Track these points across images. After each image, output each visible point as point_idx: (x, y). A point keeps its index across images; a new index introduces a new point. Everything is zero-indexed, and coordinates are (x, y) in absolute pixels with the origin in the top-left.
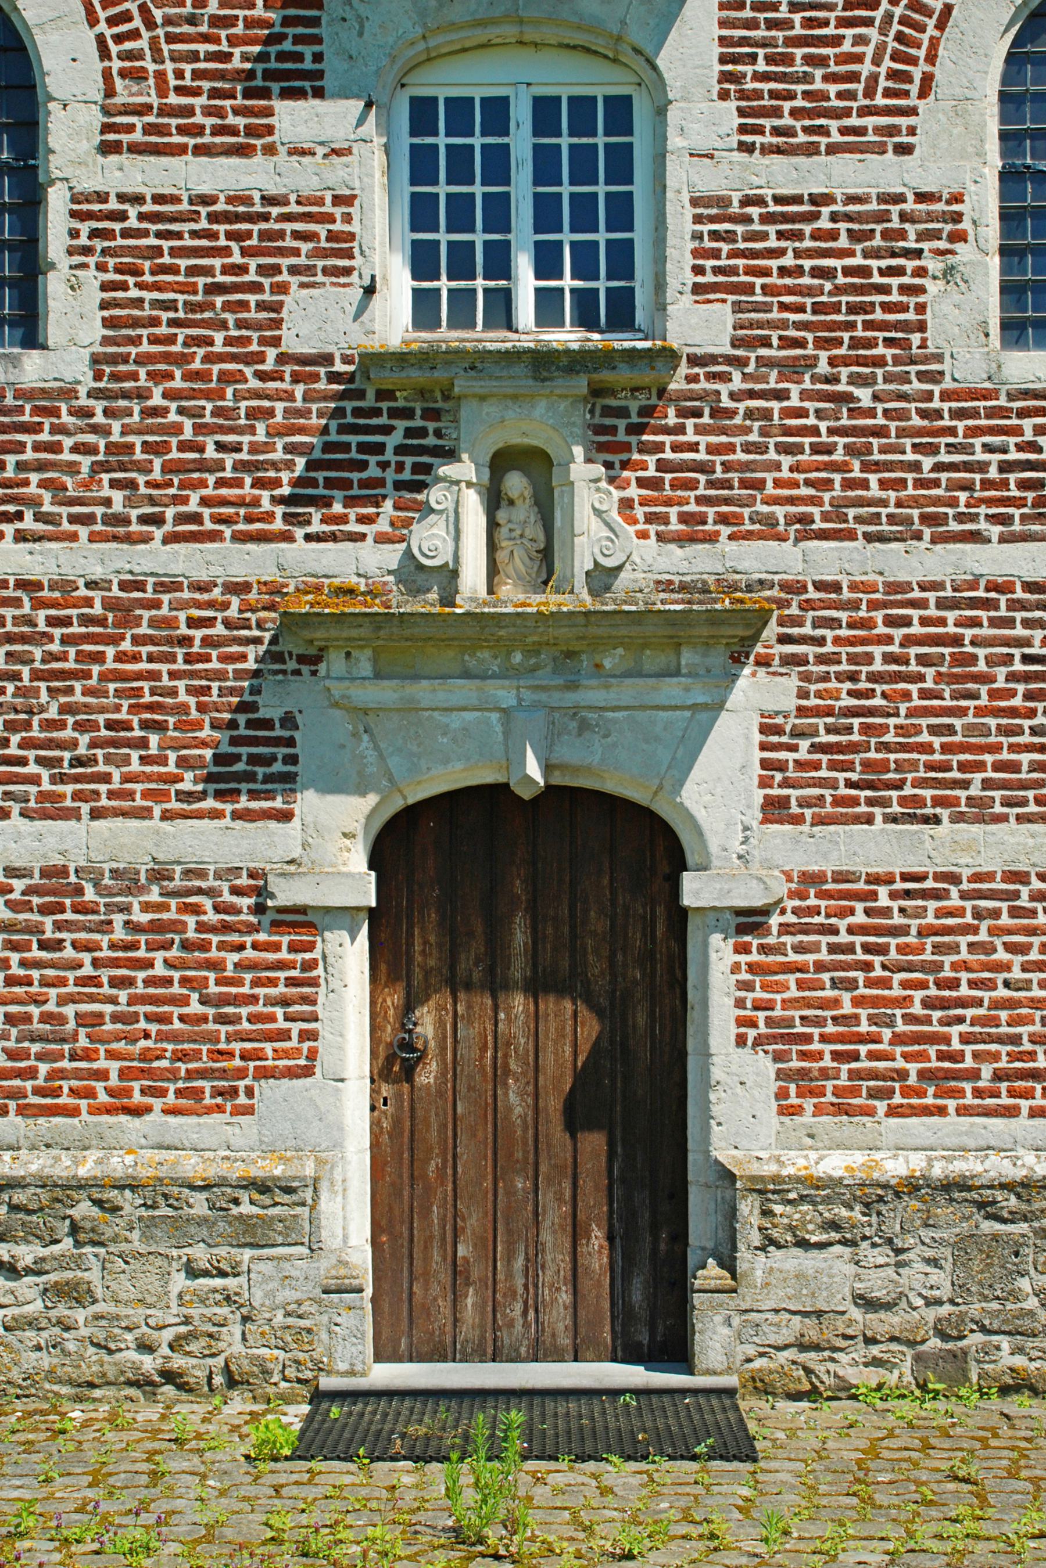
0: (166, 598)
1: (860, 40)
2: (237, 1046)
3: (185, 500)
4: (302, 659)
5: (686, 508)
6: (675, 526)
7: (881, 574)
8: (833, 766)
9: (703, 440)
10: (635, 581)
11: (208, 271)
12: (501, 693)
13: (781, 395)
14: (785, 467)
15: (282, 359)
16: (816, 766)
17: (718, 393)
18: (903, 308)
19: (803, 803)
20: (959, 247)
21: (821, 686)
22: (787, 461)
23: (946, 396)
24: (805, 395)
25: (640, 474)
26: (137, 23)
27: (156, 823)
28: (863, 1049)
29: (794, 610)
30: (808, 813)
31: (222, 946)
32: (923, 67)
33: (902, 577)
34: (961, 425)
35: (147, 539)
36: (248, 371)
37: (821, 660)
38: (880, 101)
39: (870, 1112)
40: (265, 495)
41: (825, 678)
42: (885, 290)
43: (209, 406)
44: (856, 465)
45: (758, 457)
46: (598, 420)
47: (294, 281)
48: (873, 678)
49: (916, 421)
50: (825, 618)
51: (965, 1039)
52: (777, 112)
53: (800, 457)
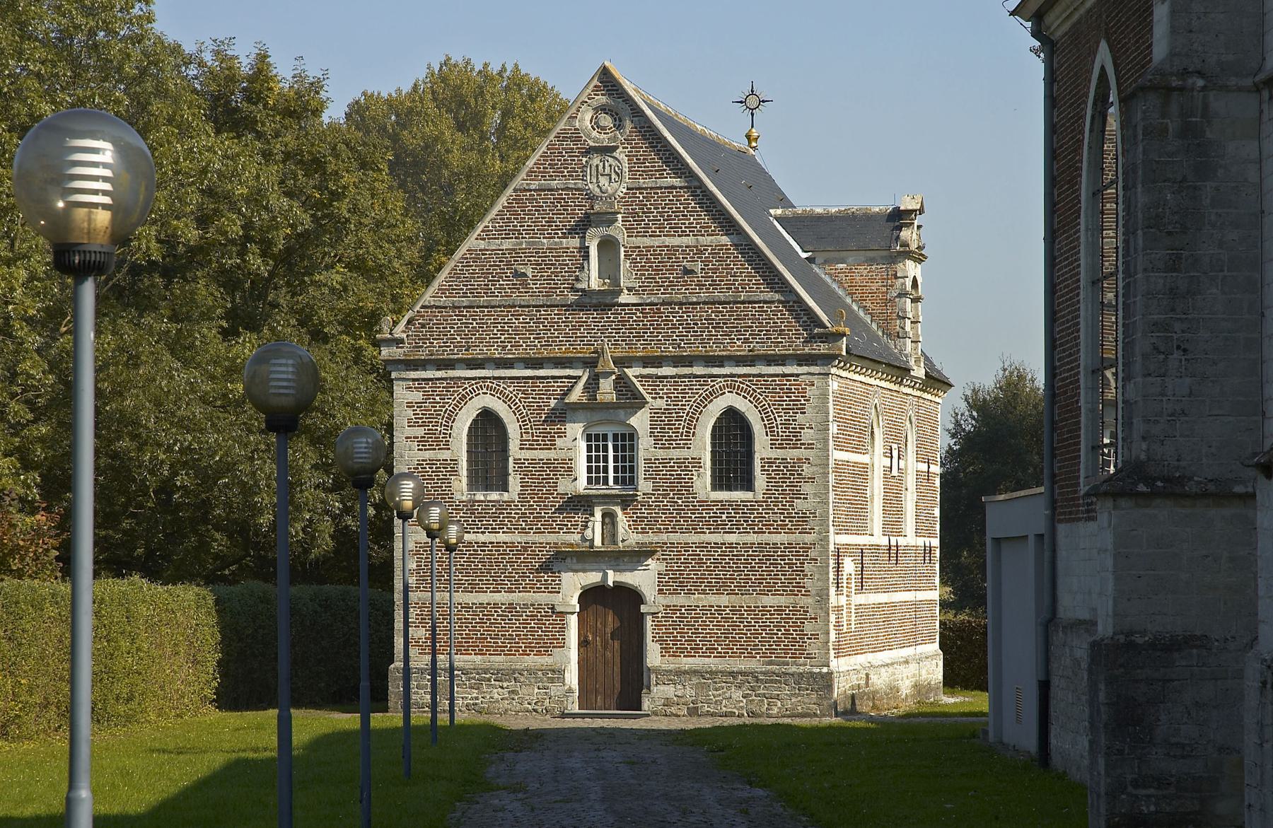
6: (640, 530)
18: (688, 483)
22: (663, 516)
24: (667, 502)
27: (532, 594)
37: (670, 559)
38: (684, 438)
42: (685, 479)
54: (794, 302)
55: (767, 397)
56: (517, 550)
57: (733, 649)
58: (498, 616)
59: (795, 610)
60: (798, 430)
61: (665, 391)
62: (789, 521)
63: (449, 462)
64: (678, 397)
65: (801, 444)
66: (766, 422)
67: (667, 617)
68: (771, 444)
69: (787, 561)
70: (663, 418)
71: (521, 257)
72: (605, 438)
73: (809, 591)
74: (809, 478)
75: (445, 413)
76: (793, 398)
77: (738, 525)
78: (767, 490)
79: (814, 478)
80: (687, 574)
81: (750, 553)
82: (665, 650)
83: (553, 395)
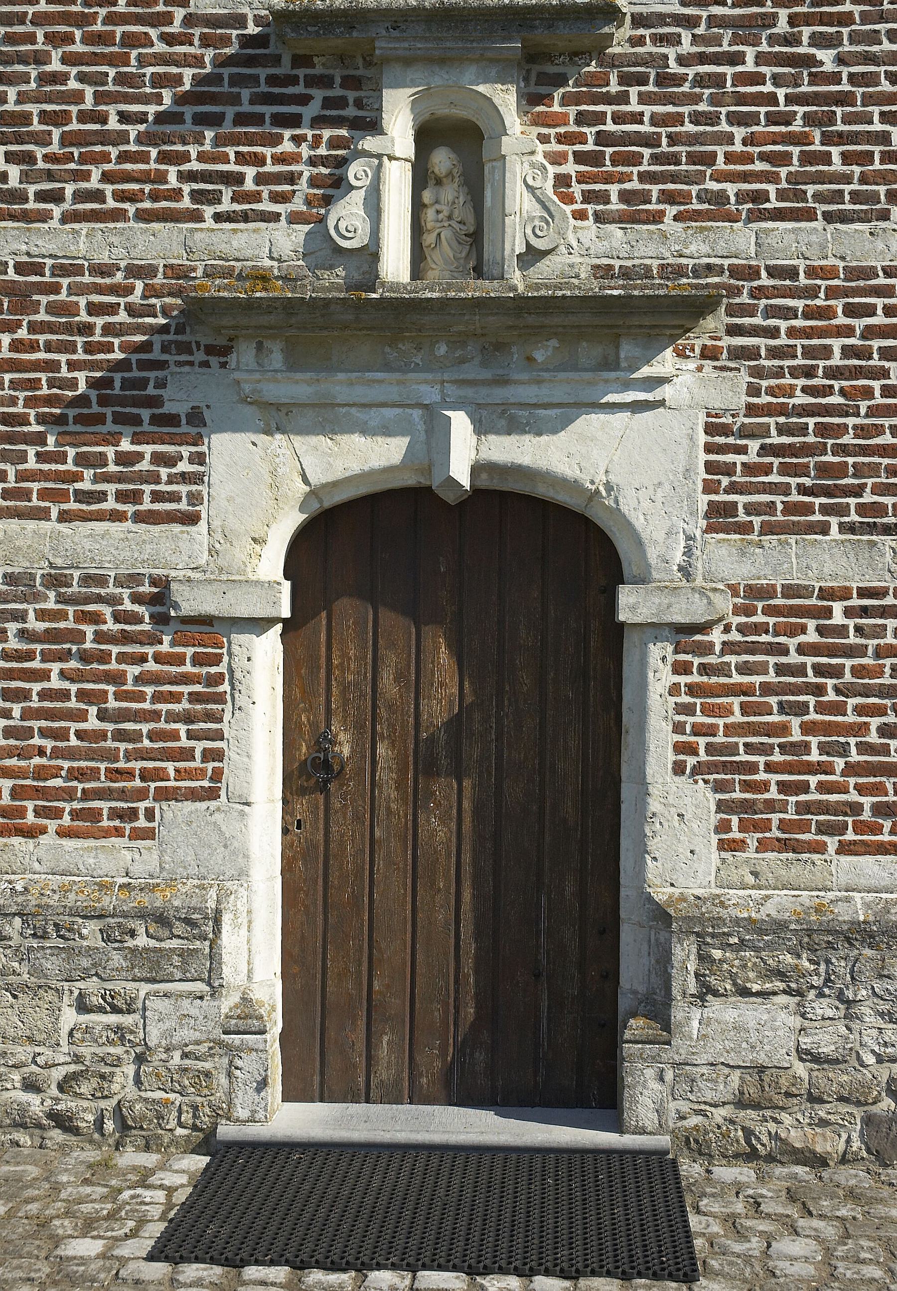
0: (65, 282)
2: (137, 765)
3: (86, 176)
4: (210, 350)
5: (627, 186)
6: (615, 205)
7: (843, 258)
8: (785, 470)
9: (648, 110)
10: (571, 266)
12: (424, 388)
13: (736, 59)
14: (738, 140)
15: (189, 20)
17: (666, 57)
19: (751, 509)
21: (773, 382)
22: (739, 133)
24: (760, 59)
25: (578, 147)
28: (813, 780)
29: (745, 299)
30: (757, 521)
31: (122, 658)
35: (45, 216)
36: (153, 33)
37: (775, 353)
39: (820, 848)
40: (172, 172)
41: (779, 373)
43: (112, 72)
44: (817, 135)
45: (708, 129)
46: (533, 89)
48: (833, 373)
50: (779, 307)
53: (755, 128)
67: (752, 649)
80: (862, 431)
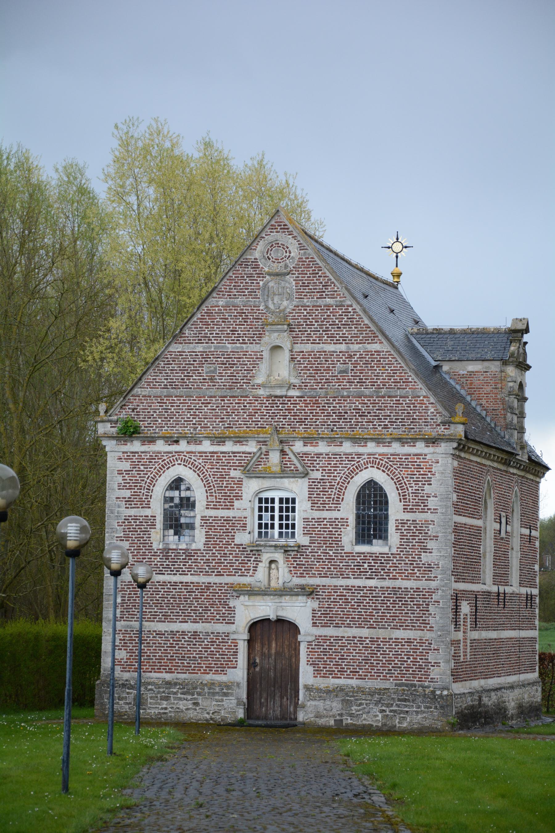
1: (332, 491)
2: (224, 663)
4: (237, 597)
9: (304, 560)
11: (223, 529)
16: (321, 617)
18: (338, 538)
20: (347, 527)
22: (318, 564)
23: (345, 553)
26: (212, 487)
31: (223, 645)
32: (342, 496)
33: (336, 585)
34: (347, 558)
37: (322, 599)
38: (335, 502)
39: (329, 677)
42: (335, 534)
47: (237, 531)
48: (331, 602)
49: (339, 557)
51: (345, 665)
52: (317, 503)
54: (424, 397)
55: (401, 471)
56: (201, 589)
57: (371, 672)
58: (185, 641)
59: (421, 642)
60: (425, 498)
61: (321, 465)
62: (418, 570)
63: (150, 518)
64: (331, 470)
65: (428, 509)
66: (400, 491)
68: (404, 509)
69: (415, 603)
70: (319, 487)
71: (210, 358)
72: (273, 500)
73: (433, 627)
74: (434, 536)
75: (148, 478)
76: (422, 473)
77: (377, 572)
78: (401, 545)
79: (438, 537)
81: (386, 595)
82: (317, 672)
83: (233, 466)
